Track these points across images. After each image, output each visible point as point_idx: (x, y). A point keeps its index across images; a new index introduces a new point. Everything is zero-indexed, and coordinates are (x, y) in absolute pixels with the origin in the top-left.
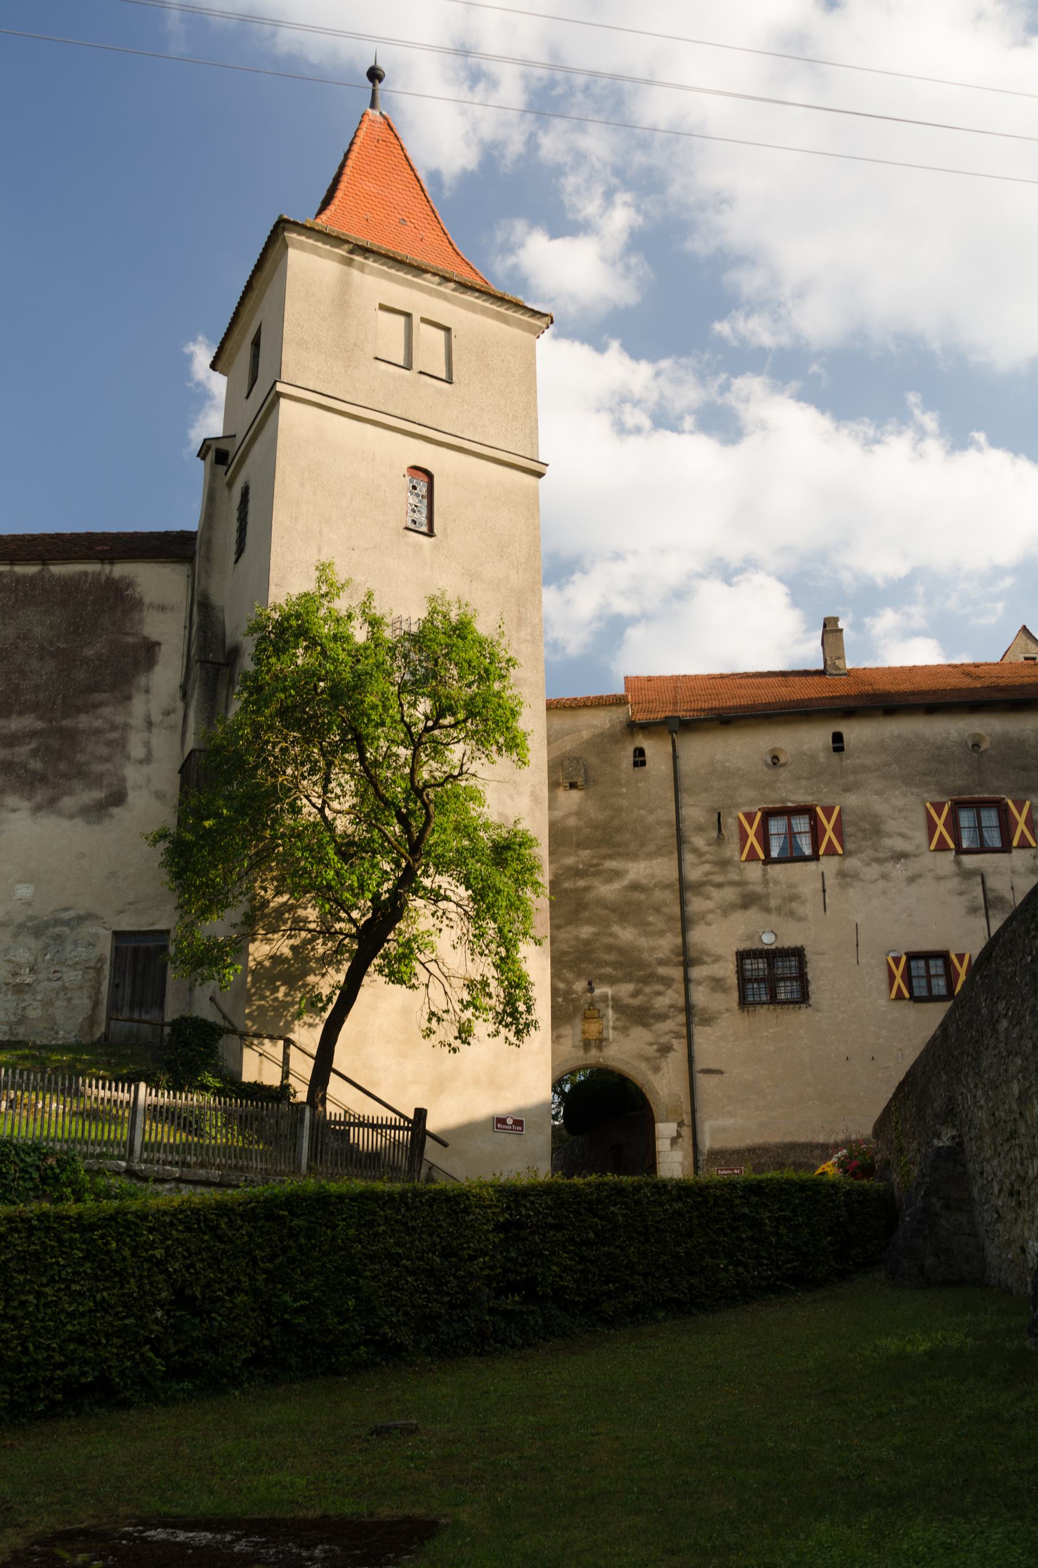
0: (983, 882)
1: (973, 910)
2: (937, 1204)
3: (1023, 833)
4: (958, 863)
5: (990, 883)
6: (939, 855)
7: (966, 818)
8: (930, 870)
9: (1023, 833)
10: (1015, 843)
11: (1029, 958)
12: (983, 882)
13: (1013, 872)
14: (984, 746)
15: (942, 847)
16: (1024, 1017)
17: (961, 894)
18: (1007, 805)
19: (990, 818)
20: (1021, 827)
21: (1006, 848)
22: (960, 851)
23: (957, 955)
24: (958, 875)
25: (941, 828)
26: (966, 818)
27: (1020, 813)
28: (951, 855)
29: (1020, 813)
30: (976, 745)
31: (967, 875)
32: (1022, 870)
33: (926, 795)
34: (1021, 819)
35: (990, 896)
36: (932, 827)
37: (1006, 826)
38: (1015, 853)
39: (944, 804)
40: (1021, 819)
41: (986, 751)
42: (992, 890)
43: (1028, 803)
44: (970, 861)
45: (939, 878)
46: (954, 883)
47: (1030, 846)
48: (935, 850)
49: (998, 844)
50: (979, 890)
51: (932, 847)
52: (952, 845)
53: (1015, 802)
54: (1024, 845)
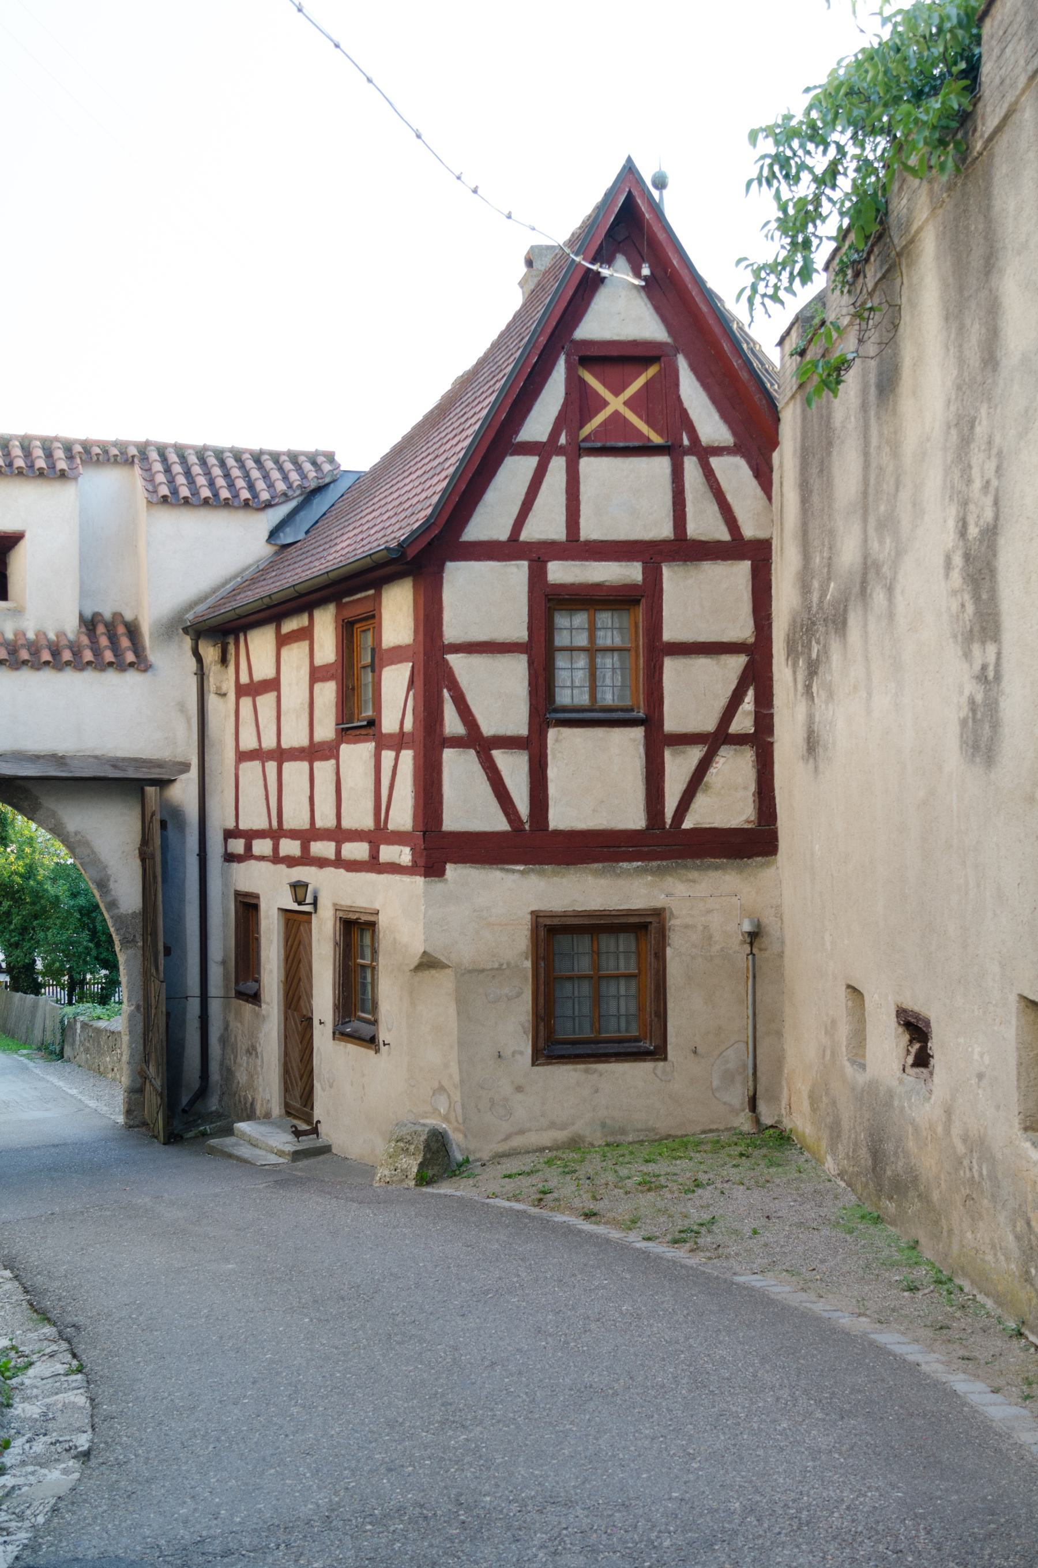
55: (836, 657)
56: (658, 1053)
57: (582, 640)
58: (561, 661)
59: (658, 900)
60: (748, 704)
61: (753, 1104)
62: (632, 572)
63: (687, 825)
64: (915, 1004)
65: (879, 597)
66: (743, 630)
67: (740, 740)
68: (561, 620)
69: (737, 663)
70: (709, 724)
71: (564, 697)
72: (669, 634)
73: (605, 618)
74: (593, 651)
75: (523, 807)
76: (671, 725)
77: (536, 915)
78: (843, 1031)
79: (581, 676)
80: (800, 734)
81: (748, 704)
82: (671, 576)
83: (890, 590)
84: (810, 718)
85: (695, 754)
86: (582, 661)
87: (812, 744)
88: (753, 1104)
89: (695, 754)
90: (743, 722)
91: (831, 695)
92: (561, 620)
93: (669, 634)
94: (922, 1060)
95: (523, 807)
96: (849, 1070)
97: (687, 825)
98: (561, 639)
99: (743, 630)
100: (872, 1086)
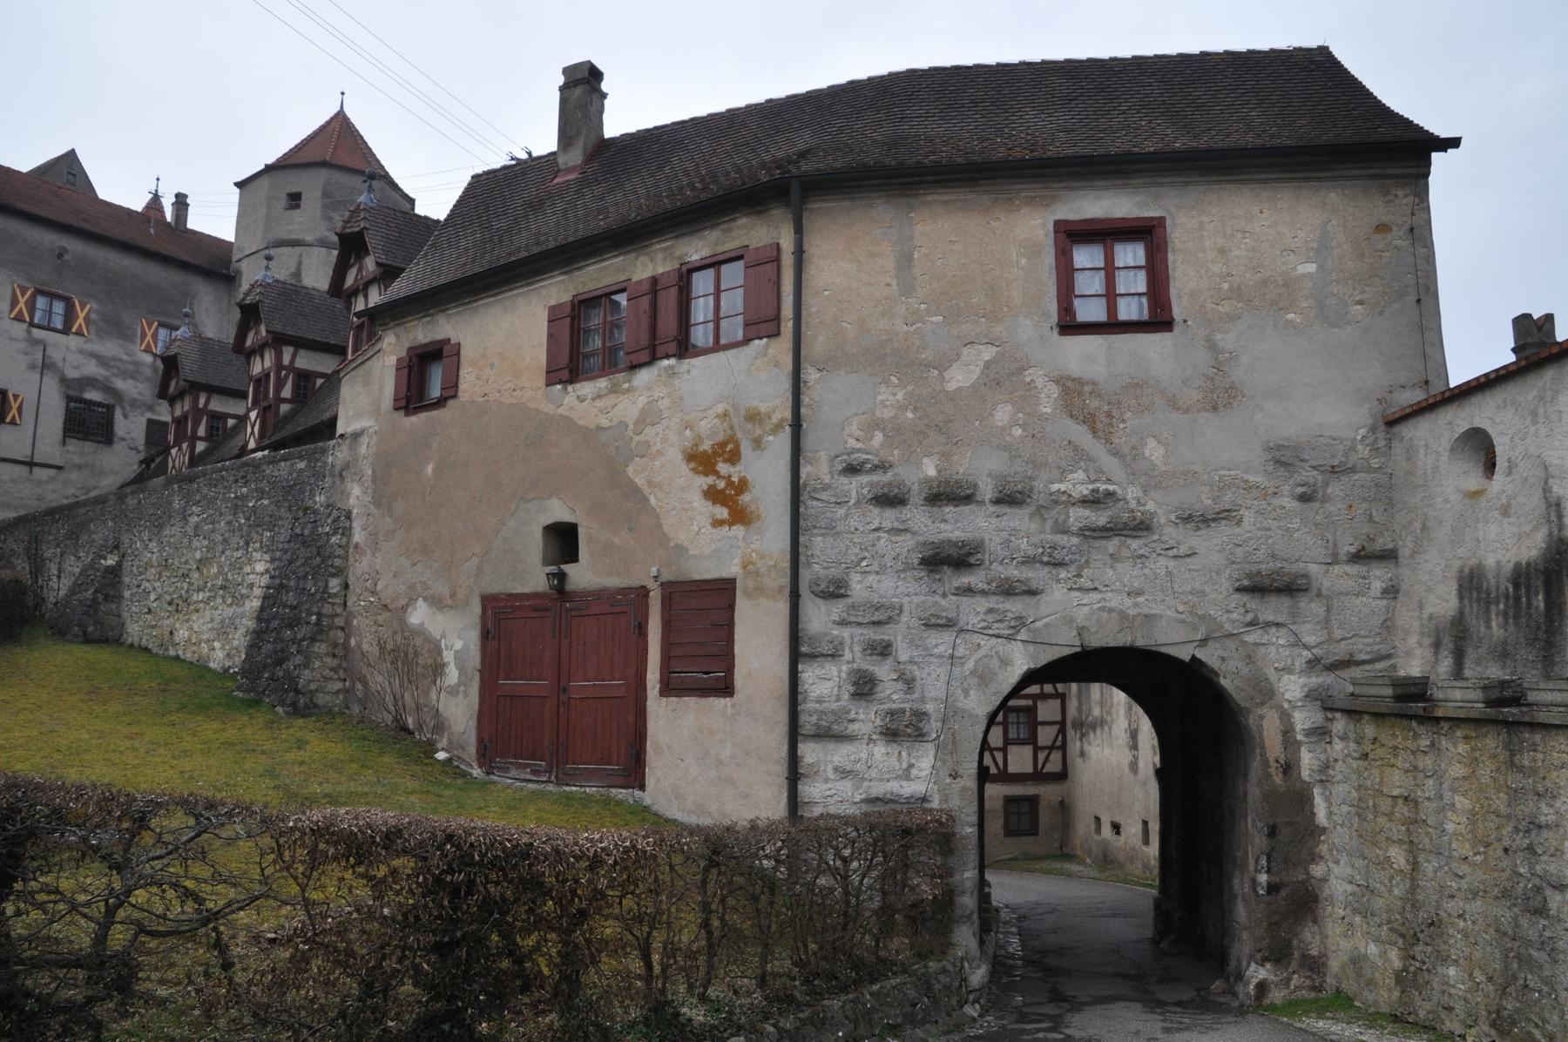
0: (44, 350)
1: (32, 367)
2: (100, 597)
3: (80, 325)
4: (29, 332)
5: (49, 351)
6: (16, 324)
7: (41, 302)
8: (6, 332)
9: (80, 325)
10: (74, 330)
11: (233, 495)
12: (44, 350)
13: (68, 349)
14: (66, 257)
15: (19, 318)
16: (219, 522)
17: (26, 354)
18: (74, 303)
19: (59, 307)
20: (80, 320)
21: (66, 331)
22: (32, 324)
23: (14, 395)
24: (26, 340)
25: (22, 305)
26: (41, 302)
27: (82, 310)
28: (25, 326)
29: (82, 310)
30: (60, 256)
31: (34, 342)
32: (74, 349)
33: (15, 278)
34: (82, 315)
35: (47, 360)
36: (14, 302)
37: (69, 316)
38: (71, 336)
39: (28, 288)
40: (82, 315)
41: (67, 261)
42: (50, 357)
43: (89, 306)
44: (37, 333)
45: (12, 339)
46: (22, 345)
47: (83, 335)
48: (14, 319)
49: (59, 326)
50: (40, 356)
51: (12, 316)
52: (28, 319)
53: (80, 302)
54: (79, 333)
55: (1092, 735)
56: (1036, 834)
57: (1015, 720)
58: (1010, 727)
59: (1037, 792)
60: (1060, 739)
61: (1061, 847)
62: (1030, 702)
63: (1044, 771)
64: (1117, 819)
65: (1106, 728)
66: (1058, 718)
67: (1058, 748)
68: (1010, 715)
69: (1057, 727)
70: (1050, 744)
71: (1011, 736)
72: (1039, 719)
73: (1022, 714)
74: (1018, 723)
75: (1001, 766)
76: (1040, 744)
77: (1005, 796)
78: (1093, 827)
79: (1015, 730)
80: (1078, 750)
81: (1060, 739)
82: (1040, 705)
83: (1110, 729)
84: (1082, 748)
85: (1047, 752)
86: (1015, 726)
87: (1083, 754)
88: (1061, 847)
89: (1047, 752)
90: (1058, 743)
91: (1089, 743)
92: (1010, 715)
93: (1039, 719)
94: (1118, 833)
95: (1001, 766)
96: (1095, 836)
97: (1044, 771)
98: (1010, 720)
99: (1058, 718)
100: (1104, 840)
